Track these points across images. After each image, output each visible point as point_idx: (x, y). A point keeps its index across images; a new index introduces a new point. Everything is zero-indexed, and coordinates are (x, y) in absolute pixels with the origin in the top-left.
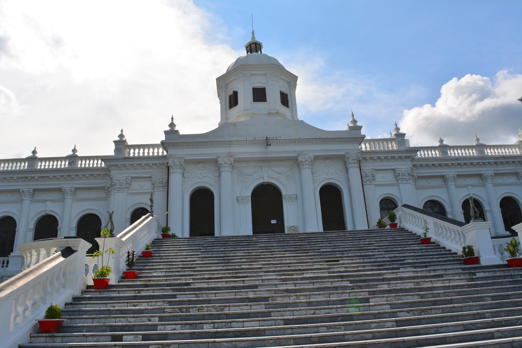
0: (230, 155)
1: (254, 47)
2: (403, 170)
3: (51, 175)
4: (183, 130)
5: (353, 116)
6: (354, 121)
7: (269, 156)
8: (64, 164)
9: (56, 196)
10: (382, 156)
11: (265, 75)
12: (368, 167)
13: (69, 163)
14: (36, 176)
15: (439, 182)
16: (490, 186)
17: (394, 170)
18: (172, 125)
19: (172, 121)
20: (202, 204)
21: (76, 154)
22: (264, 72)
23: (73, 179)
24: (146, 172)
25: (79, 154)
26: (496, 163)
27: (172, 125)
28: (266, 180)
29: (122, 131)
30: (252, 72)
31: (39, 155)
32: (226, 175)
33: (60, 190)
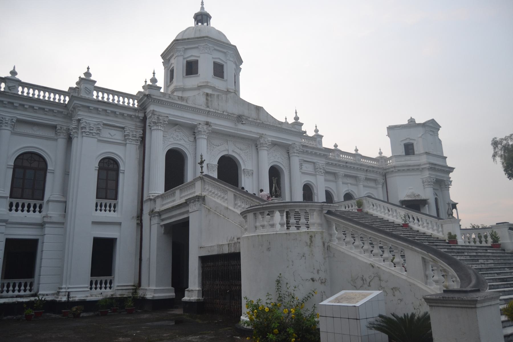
0: (207, 124)
1: (202, 18)
2: (321, 164)
5: (296, 113)
6: (297, 118)
7: (238, 132)
11: (225, 53)
13: (8, 87)
15: (331, 178)
17: (314, 163)
19: (154, 76)
21: (17, 77)
22: (225, 51)
23: (15, 108)
24: (119, 122)
26: (367, 170)
28: (231, 153)
29: (88, 68)
30: (216, 48)
32: (203, 143)
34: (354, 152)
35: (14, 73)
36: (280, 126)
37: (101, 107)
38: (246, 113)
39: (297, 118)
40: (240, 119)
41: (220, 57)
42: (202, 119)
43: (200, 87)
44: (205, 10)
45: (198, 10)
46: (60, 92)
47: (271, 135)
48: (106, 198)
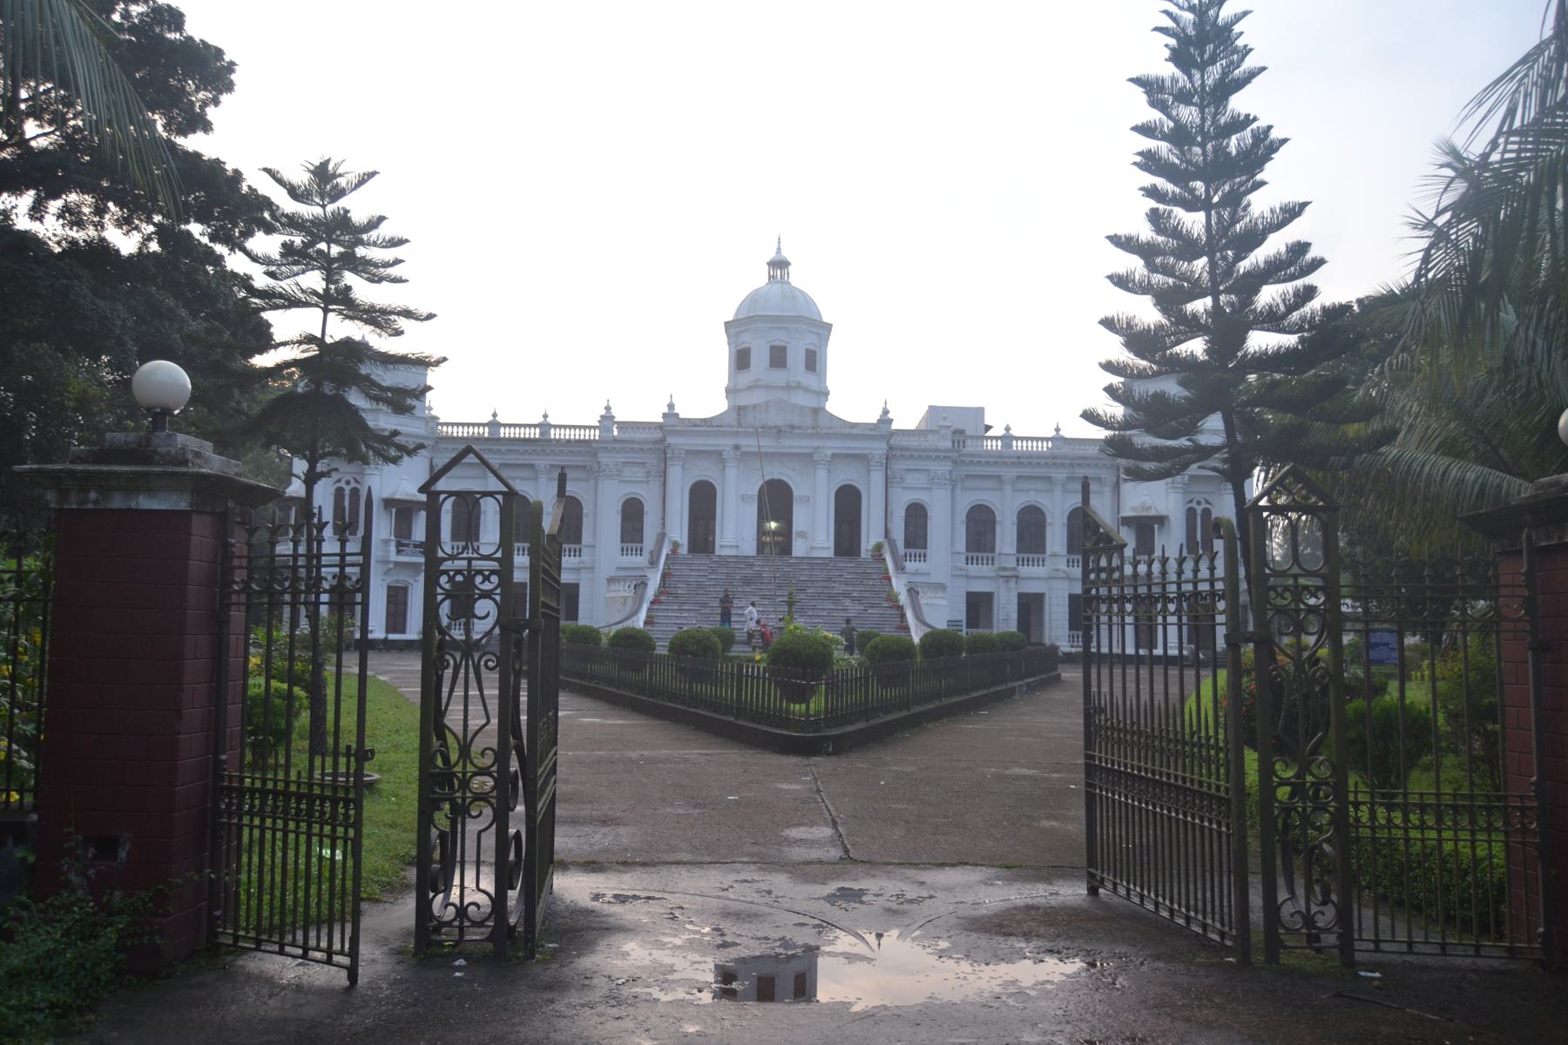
0: (737, 447)
1: (779, 264)
3: (521, 449)
4: (686, 411)
6: (886, 412)
8: (535, 433)
9: (527, 473)
10: (916, 454)
12: (898, 466)
14: (504, 448)
16: (1058, 492)
18: (671, 406)
20: (703, 500)
25: (551, 420)
27: (671, 406)
28: (776, 477)
31: (501, 419)
32: (732, 473)
33: (532, 466)
34: (1052, 434)
35: (545, 416)
36: (846, 431)
37: (618, 446)
38: (796, 422)
39: (886, 412)
40: (779, 432)
41: (779, 338)
42: (732, 441)
43: (750, 388)
44: (784, 253)
45: (771, 255)
46: (590, 427)
47: (832, 446)
48: (632, 541)
